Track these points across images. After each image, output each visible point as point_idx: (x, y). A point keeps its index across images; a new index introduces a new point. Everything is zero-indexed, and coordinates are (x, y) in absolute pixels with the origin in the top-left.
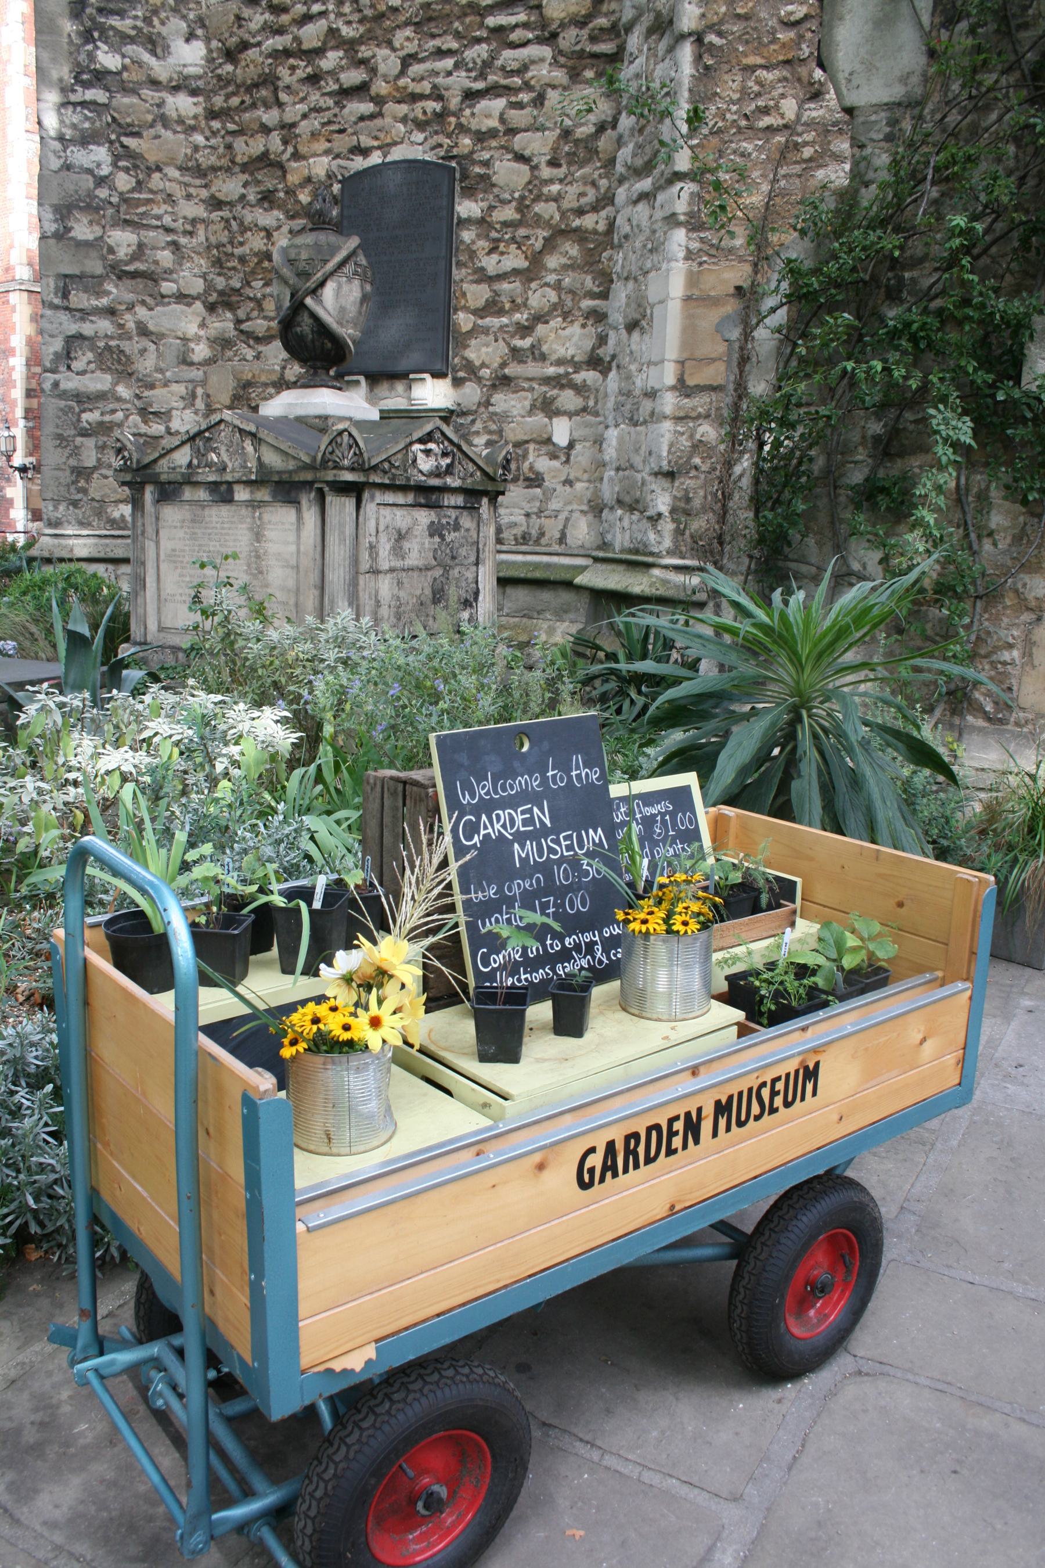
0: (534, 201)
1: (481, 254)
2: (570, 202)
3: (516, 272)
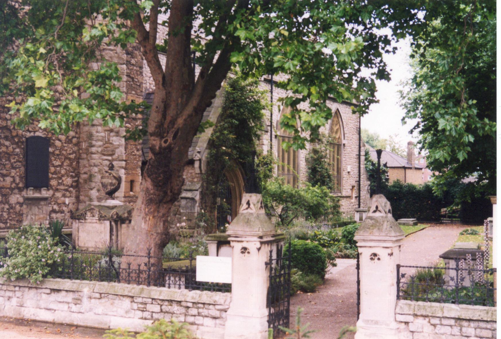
2: (68, 152)
3: (59, 165)
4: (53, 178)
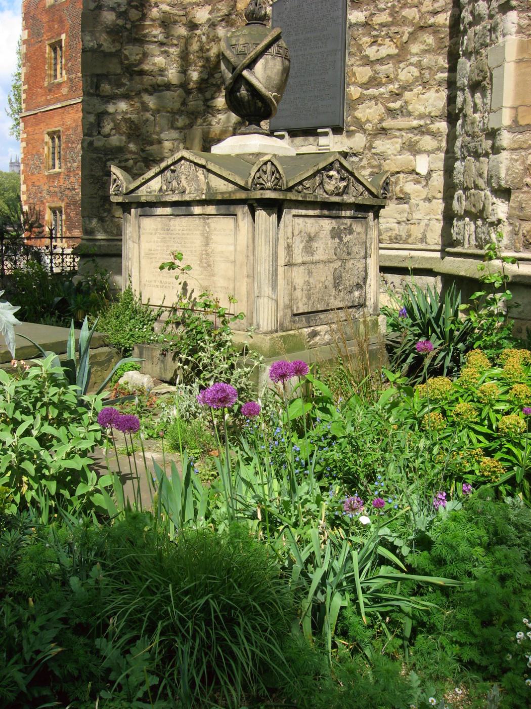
0: (401, 8)
1: (365, 46)
4: (361, 100)
